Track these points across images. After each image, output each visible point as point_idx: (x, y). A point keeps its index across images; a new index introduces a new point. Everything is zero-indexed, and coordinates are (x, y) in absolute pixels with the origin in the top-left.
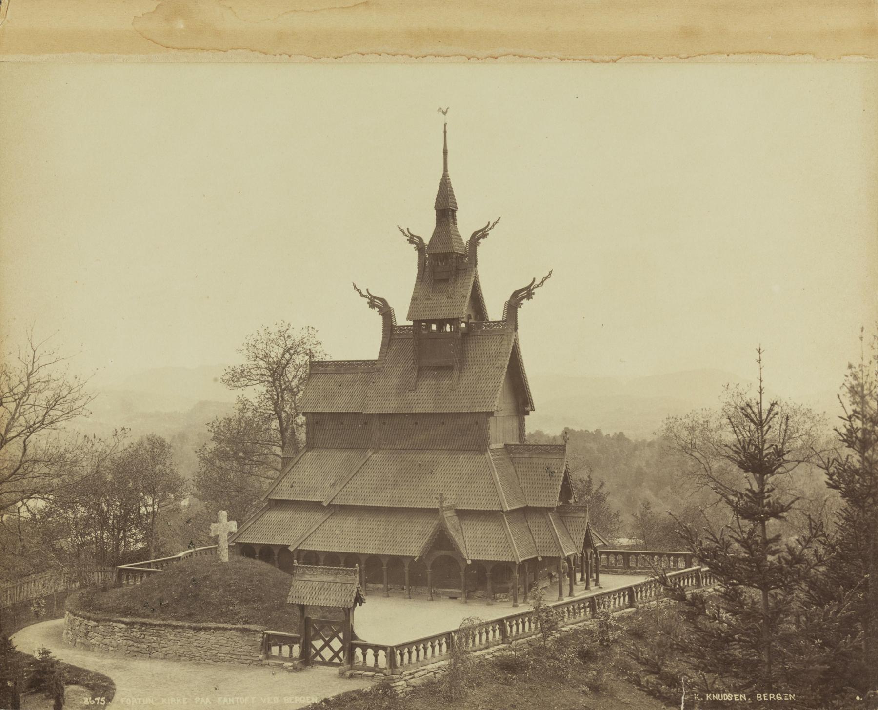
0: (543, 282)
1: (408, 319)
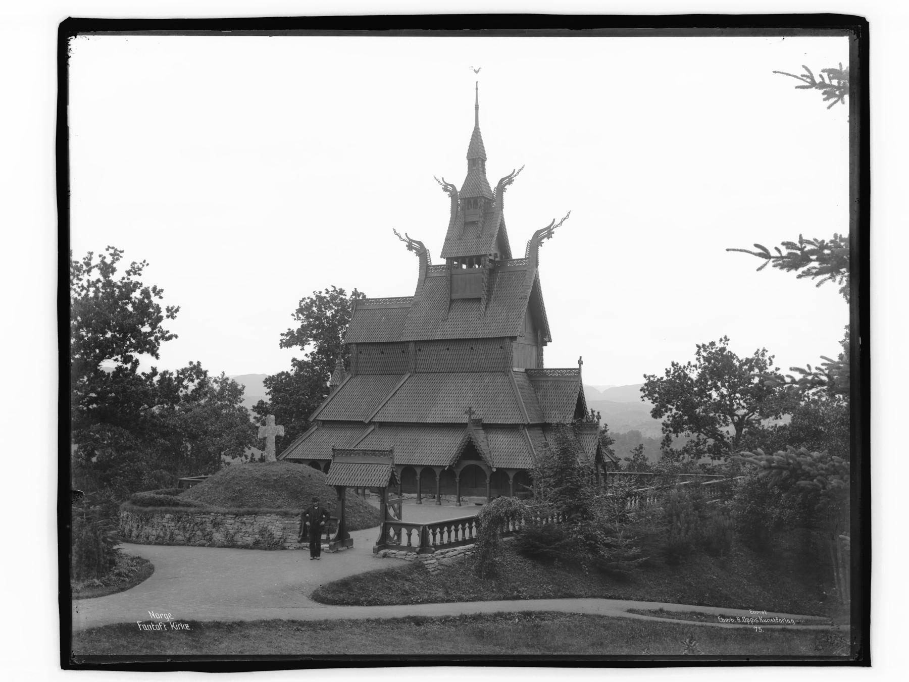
0: (562, 222)
1: (442, 257)
